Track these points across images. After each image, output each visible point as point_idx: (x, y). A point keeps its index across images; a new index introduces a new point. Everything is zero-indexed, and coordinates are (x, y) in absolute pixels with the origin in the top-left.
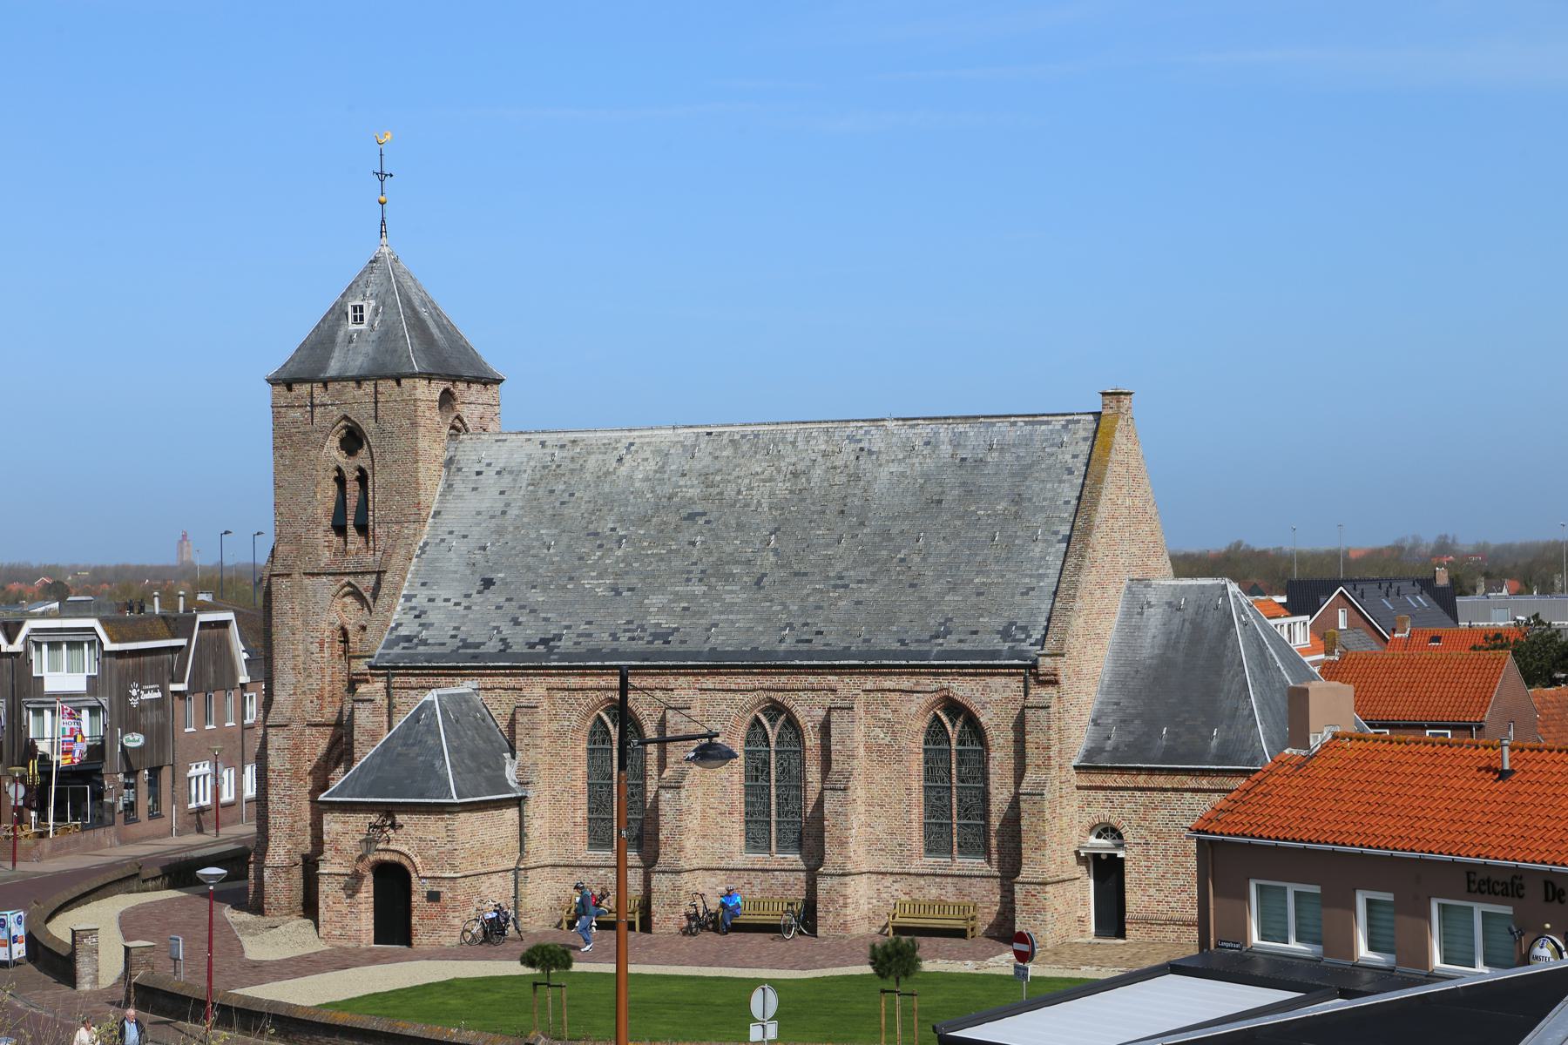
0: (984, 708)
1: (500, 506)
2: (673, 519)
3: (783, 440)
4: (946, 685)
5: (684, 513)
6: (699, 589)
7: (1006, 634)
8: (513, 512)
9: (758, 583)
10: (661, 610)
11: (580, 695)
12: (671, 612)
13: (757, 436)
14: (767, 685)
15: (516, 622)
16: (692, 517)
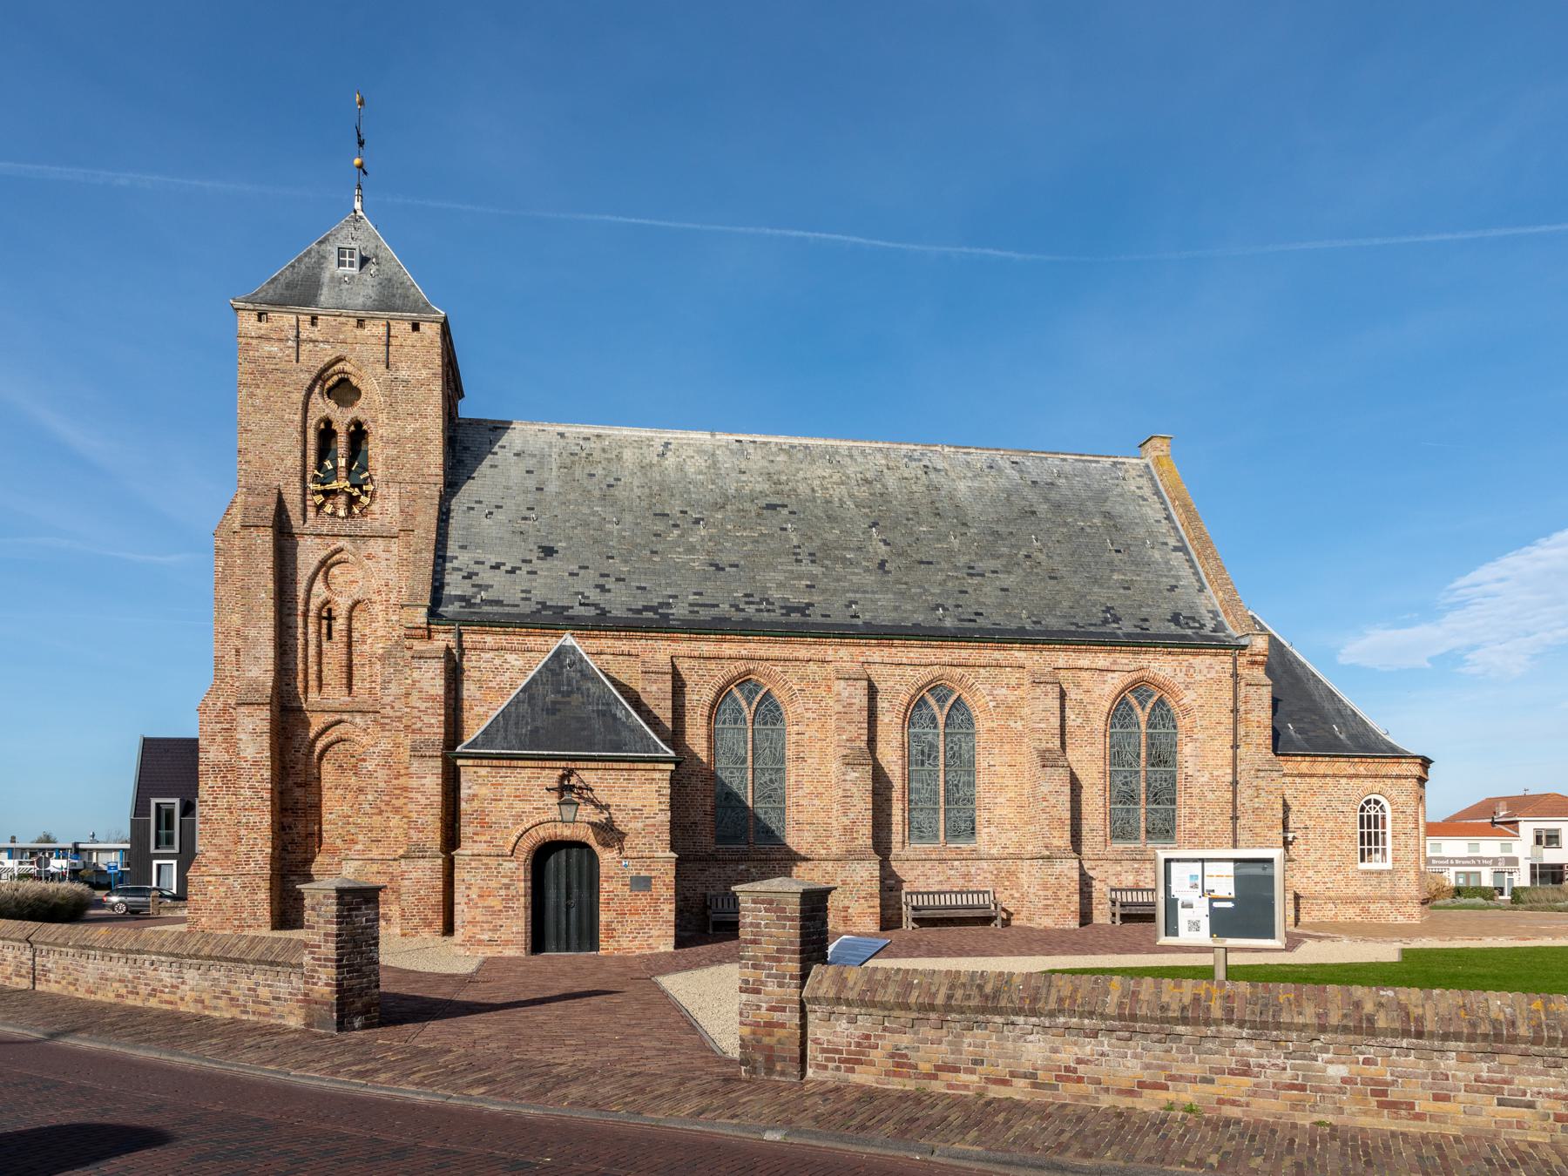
0: (1187, 688)
1: (531, 483)
2: (753, 509)
3: (837, 452)
4: (1145, 664)
5: (763, 502)
6: (816, 570)
8: (552, 488)
9: (882, 564)
10: (780, 585)
11: (712, 665)
12: (794, 589)
13: (807, 447)
14: (946, 659)
15: (602, 588)
16: (772, 507)
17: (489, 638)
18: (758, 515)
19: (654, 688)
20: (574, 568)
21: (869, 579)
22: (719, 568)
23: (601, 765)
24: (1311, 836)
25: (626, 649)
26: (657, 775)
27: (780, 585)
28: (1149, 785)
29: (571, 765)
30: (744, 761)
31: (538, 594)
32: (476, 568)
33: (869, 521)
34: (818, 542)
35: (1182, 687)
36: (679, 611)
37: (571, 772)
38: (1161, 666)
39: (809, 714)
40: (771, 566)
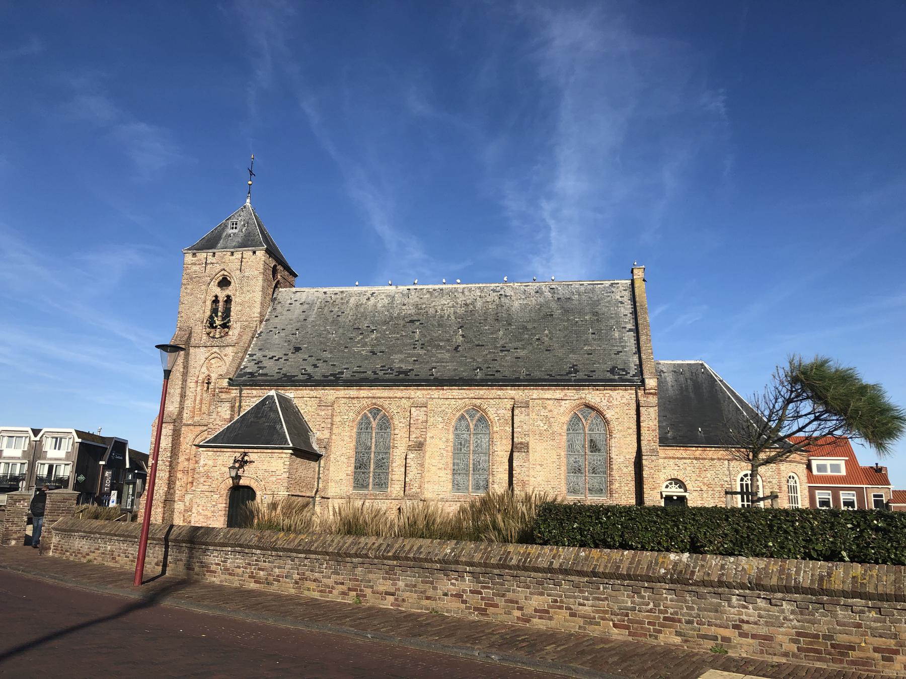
0: (608, 408)
1: (302, 317)
2: (402, 322)
3: (457, 291)
4: (583, 396)
5: (407, 320)
6: (422, 352)
7: (612, 371)
8: (311, 319)
9: (456, 349)
10: (401, 361)
11: (355, 401)
13: (442, 290)
15: (315, 366)
16: (412, 321)
17: (254, 392)
18: (404, 326)
19: (323, 413)
20: (306, 357)
21: (447, 356)
22: (374, 353)
23: (259, 450)
24: (705, 495)
25: (315, 395)
26: (284, 455)
27: (401, 361)
28: (590, 463)
29: (246, 450)
30: (370, 448)
31: (284, 371)
32: (262, 359)
33: (459, 326)
34: (429, 338)
35: (605, 408)
36: (346, 375)
37: (245, 454)
38: (593, 396)
39: (401, 425)
40: (401, 352)
